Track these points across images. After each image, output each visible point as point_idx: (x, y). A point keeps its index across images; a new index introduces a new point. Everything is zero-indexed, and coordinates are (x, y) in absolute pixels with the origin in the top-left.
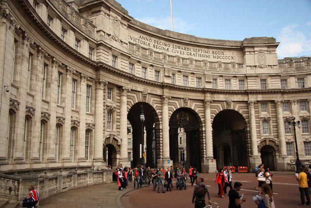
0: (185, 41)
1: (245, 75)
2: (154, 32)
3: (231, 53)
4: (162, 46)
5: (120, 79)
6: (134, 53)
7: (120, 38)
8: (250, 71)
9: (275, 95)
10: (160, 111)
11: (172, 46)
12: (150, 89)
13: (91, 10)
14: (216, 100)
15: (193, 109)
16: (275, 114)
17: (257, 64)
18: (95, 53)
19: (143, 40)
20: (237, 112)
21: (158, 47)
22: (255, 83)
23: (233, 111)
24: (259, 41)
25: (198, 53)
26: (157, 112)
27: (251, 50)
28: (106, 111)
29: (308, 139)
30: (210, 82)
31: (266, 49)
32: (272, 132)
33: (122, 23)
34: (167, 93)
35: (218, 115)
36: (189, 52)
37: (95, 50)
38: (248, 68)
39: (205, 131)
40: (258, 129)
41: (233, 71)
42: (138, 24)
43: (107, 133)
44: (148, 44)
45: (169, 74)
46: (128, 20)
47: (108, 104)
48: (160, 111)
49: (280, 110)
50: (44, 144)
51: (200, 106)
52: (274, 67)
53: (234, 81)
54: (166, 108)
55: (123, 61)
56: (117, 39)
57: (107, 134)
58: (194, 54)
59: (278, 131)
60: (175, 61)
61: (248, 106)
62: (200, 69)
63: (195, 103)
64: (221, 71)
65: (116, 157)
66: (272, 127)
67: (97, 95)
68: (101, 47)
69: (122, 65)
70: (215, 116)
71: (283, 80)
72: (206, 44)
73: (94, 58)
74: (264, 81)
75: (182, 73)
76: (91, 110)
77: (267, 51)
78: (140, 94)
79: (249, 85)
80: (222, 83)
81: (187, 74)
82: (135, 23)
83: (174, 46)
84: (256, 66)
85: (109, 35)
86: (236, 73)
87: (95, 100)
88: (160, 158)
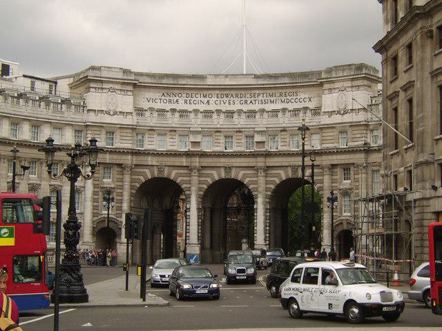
7: (119, 110)
10: (188, 186)
16: (357, 184)
17: (336, 109)
27: (331, 86)
28: (100, 193)
31: (348, 84)
36: (243, 99)
46: (135, 85)
48: (188, 186)
55: (123, 134)
58: (251, 102)
63: (244, 172)
68: (89, 128)
69: (119, 144)
78: (155, 168)
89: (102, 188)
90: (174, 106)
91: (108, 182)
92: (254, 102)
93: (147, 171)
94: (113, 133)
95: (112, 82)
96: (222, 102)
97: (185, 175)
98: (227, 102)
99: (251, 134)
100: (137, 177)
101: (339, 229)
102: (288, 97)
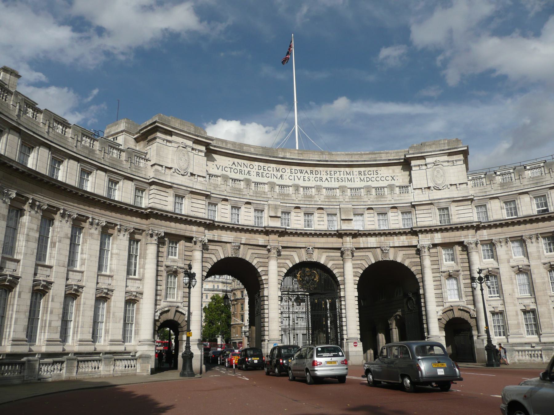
0: (311, 160)
1: (411, 203)
2: (257, 155)
3: (391, 171)
4: (272, 172)
5: (188, 227)
6: (217, 189)
7: (190, 170)
9: (465, 232)
10: (265, 269)
11: (289, 171)
12: (244, 238)
13: (147, 138)
14: (362, 246)
15: (322, 262)
18: (147, 196)
19: (239, 168)
20: (400, 266)
21: (264, 174)
22: (430, 215)
23: (394, 263)
24: (434, 146)
25: (333, 176)
26: (259, 270)
29: (529, 306)
30: (351, 220)
31: (446, 158)
32: (463, 296)
33: (196, 150)
34: (274, 241)
35: (366, 271)
36: (319, 176)
37: (147, 191)
38: (417, 191)
39: (344, 297)
40: (439, 291)
41: (390, 199)
42: (229, 146)
43: (165, 304)
44: (246, 173)
45: (276, 213)
46: (207, 145)
47: (169, 263)
48: (265, 269)
50: (42, 320)
52: (462, 186)
53: (393, 214)
56: (182, 172)
58: (327, 179)
60: (291, 193)
61: (419, 254)
62: (333, 200)
64: (370, 199)
65: (182, 338)
66: (462, 286)
70: (361, 272)
71: (481, 206)
72: (346, 161)
73: (145, 202)
75: (303, 209)
76: (139, 274)
77: (448, 162)
78: (228, 245)
80: (372, 219)
81: (310, 211)
82: (224, 146)
83: (293, 171)
84: (429, 188)
85: (171, 168)
86: (397, 202)
87: (145, 258)
88: (264, 340)
89: (167, 267)
90: (248, 177)
92: (329, 179)
94: (182, 197)
96: (296, 177)
97: (261, 256)
98: (302, 178)
99: (333, 211)
101: (450, 315)
102: (368, 176)
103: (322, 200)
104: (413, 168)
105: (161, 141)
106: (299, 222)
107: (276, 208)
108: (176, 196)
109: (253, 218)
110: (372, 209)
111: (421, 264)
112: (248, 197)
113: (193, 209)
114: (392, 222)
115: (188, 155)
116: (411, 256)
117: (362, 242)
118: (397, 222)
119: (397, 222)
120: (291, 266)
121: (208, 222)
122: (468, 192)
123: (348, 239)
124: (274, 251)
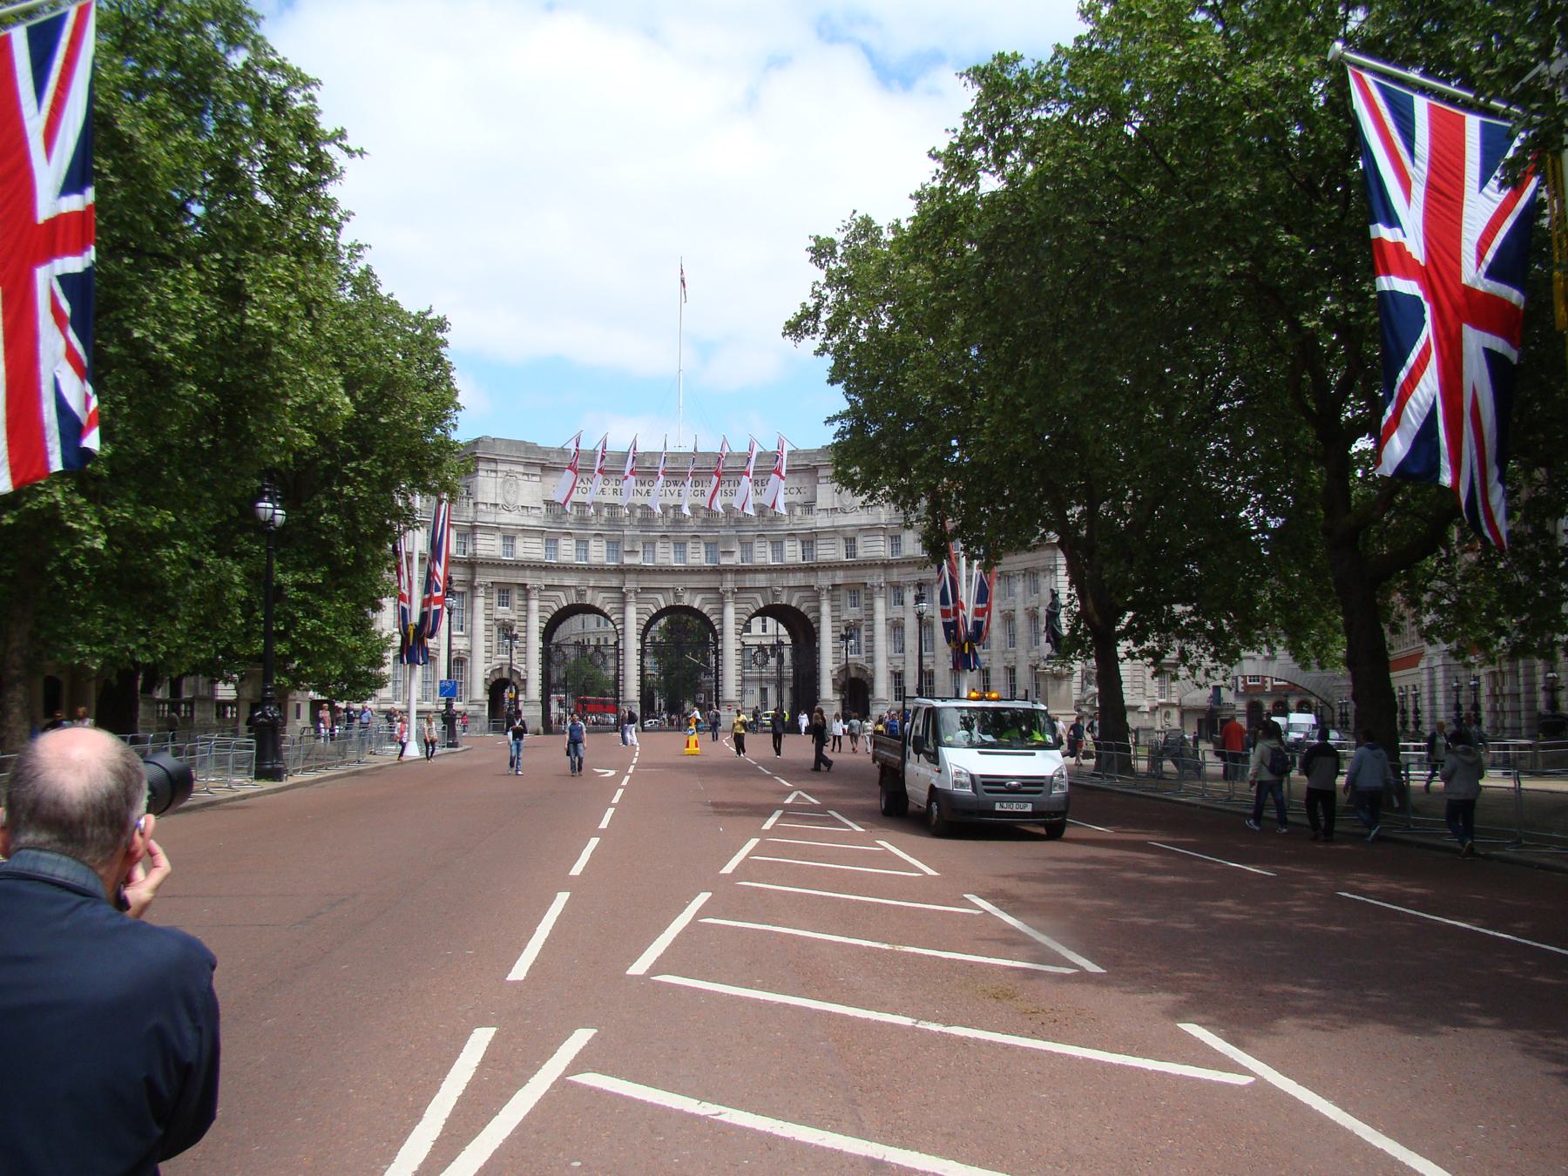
5: (521, 573)
8: (821, 521)
9: (869, 572)
10: (620, 616)
14: (748, 586)
15: (696, 607)
28: (495, 629)
32: (863, 651)
33: (528, 475)
34: (631, 584)
36: (699, 488)
45: (633, 546)
48: (620, 616)
49: (880, 604)
51: (715, 601)
53: (790, 543)
54: (631, 612)
55: (527, 540)
57: (495, 663)
59: (871, 649)
61: (818, 597)
66: (863, 639)
67: (475, 605)
70: (746, 618)
74: (851, 543)
79: (819, 552)
80: (763, 549)
85: (496, 505)
86: (796, 527)
91: (503, 613)
93: (561, 594)
94: (513, 538)
95: (512, 462)
99: (714, 540)
100: (547, 604)
103: (699, 524)
104: (821, 481)
105: (484, 473)
106: (666, 555)
107: (634, 539)
108: (505, 538)
109: (605, 554)
110: (763, 535)
111: (817, 610)
112: (598, 527)
113: (526, 550)
114: (787, 554)
115: (517, 485)
116: (809, 599)
117: (748, 581)
118: (794, 554)
119: (794, 554)
120: (655, 611)
121: (544, 565)
122: (879, 518)
123: (729, 576)
124: (632, 595)
